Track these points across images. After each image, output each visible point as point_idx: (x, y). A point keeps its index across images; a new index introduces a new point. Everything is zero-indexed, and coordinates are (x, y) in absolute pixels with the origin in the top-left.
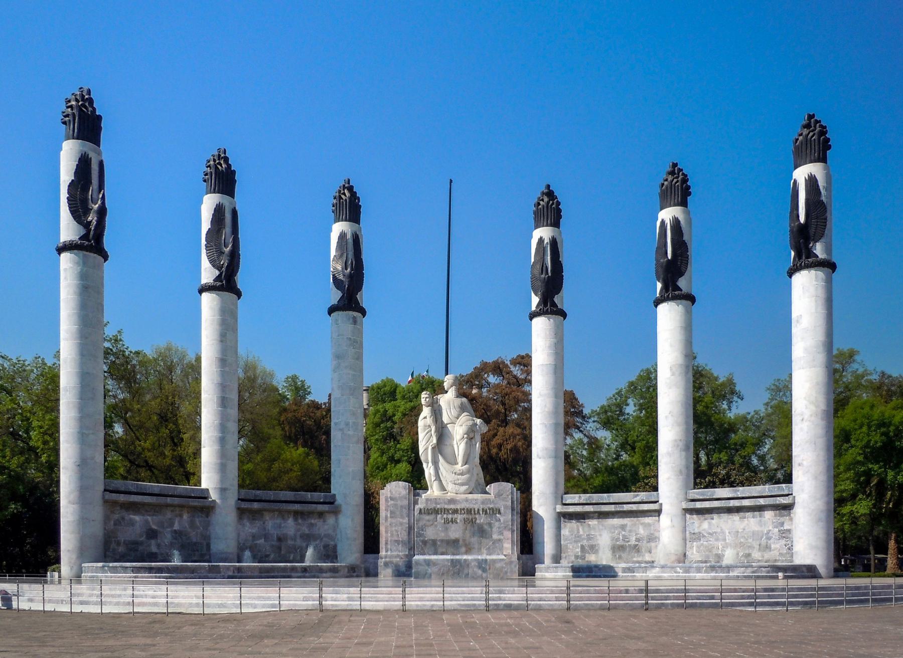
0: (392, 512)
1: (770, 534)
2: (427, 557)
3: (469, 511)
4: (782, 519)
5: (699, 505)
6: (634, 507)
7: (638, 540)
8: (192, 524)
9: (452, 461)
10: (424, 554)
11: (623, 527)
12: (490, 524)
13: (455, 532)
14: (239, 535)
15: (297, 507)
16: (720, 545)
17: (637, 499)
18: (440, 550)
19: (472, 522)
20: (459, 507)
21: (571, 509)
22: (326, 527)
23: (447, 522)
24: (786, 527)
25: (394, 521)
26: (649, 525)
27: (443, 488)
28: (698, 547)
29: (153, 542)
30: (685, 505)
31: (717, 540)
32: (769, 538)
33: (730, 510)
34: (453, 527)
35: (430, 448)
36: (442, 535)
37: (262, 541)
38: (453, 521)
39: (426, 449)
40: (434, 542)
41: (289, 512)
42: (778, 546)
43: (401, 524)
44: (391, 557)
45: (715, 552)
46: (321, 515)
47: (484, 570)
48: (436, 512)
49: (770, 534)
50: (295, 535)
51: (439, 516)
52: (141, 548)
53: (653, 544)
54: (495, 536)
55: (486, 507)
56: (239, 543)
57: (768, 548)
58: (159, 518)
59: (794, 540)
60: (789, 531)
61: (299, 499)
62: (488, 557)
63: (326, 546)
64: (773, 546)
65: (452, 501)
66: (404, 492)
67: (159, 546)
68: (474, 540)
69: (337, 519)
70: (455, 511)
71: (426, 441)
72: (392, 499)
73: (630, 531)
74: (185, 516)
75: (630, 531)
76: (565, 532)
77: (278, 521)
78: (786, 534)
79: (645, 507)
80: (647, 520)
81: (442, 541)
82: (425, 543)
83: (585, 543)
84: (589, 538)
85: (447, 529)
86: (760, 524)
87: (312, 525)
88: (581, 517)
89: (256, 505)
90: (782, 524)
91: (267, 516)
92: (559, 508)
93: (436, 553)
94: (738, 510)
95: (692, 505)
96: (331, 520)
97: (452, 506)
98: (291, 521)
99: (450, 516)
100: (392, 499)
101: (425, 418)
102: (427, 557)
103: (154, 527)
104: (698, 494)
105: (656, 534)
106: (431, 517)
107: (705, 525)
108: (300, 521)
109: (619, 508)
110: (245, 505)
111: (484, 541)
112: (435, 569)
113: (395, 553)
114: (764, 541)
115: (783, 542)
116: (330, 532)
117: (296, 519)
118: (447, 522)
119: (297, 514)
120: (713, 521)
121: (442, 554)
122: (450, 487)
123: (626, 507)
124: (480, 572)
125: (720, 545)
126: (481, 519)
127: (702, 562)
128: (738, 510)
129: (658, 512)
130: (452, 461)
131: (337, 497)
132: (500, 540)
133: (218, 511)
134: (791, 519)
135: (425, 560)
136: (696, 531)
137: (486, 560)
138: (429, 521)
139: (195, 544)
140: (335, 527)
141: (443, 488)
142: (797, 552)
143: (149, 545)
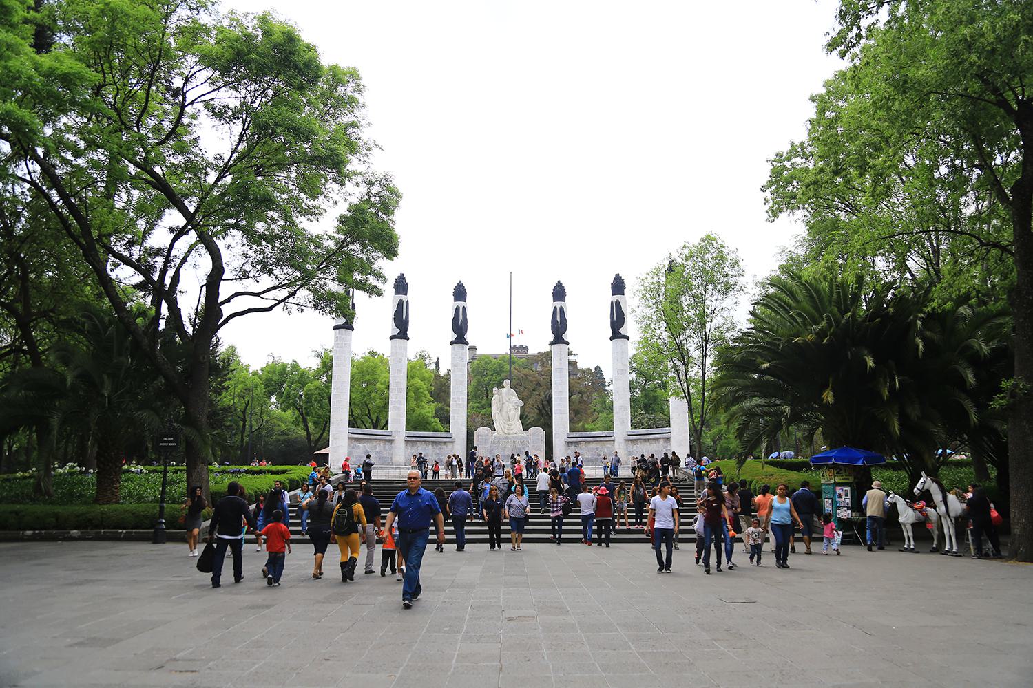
3: (514, 442)
8: (384, 447)
11: (597, 449)
14: (405, 453)
39: (495, 414)
41: (429, 442)
58: (370, 445)
71: (494, 410)
72: (481, 436)
77: (425, 446)
79: (607, 439)
80: (609, 445)
88: (577, 444)
89: (414, 439)
94: (649, 439)
96: (450, 446)
98: (430, 446)
100: (481, 436)
110: (409, 439)
117: (433, 446)
129: (614, 441)
133: (396, 441)
134: (670, 444)
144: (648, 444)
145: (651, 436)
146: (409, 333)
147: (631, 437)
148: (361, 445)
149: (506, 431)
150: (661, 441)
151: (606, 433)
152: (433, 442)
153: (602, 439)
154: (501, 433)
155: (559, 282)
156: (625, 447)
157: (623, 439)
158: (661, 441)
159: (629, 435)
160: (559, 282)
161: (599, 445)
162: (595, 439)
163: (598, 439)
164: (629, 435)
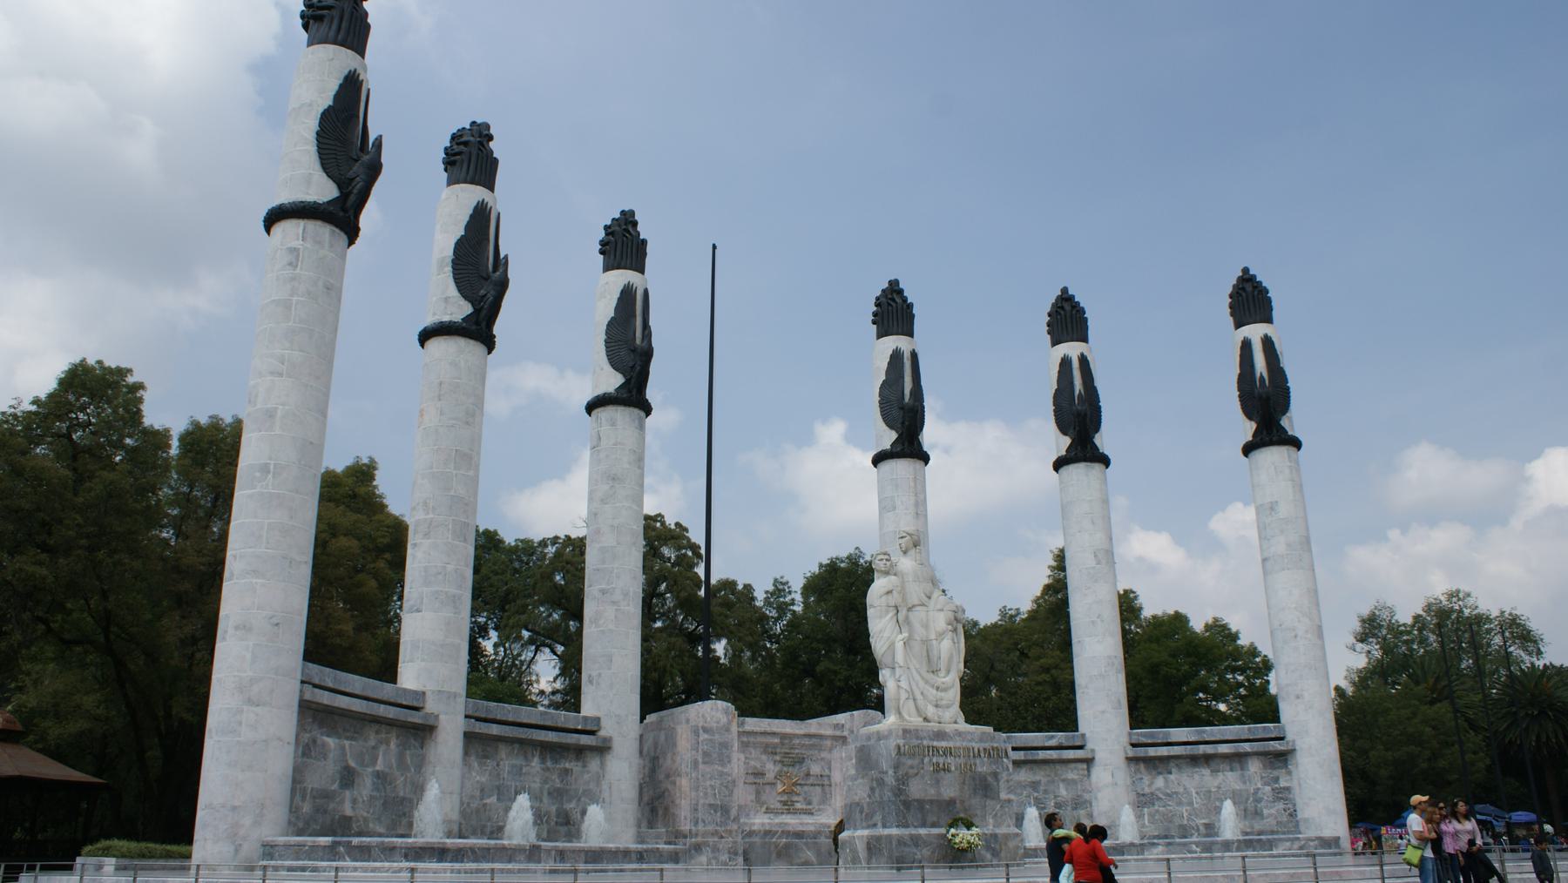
0: (706, 754)
1: (1260, 795)
2: (913, 831)
4: (1276, 773)
5: (1152, 752)
6: (1053, 754)
7: (1058, 805)
10: (906, 826)
12: (995, 775)
13: (949, 790)
15: (551, 737)
16: (1184, 810)
17: (1053, 743)
18: (931, 818)
20: (951, 744)
22: (586, 776)
24: (1283, 784)
25: (708, 769)
26: (1074, 782)
28: (1151, 815)
29: (348, 793)
30: (1131, 752)
31: (1180, 803)
32: (1258, 800)
33: (1194, 760)
35: (899, 646)
36: (932, 793)
37: (493, 799)
38: (946, 770)
39: (892, 646)
40: (921, 803)
42: (1273, 811)
43: (721, 774)
44: (705, 834)
45: (1177, 821)
46: (580, 752)
47: (996, 854)
49: (1260, 795)
50: (541, 790)
51: (926, 760)
52: (331, 806)
53: (1082, 812)
54: (1003, 796)
55: (987, 745)
56: (462, 803)
57: (1257, 814)
59: (1299, 801)
60: (1288, 789)
61: (548, 723)
62: (997, 831)
64: (1265, 812)
66: (724, 720)
67: (354, 801)
68: (976, 801)
69: (602, 765)
70: (948, 752)
72: (705, 730)
73: (1046, 792)
74: (393, 746)
75: (1046, 792)
77: (519, 761)
78: (1282, 794)
79: (1071, 754)
80: (1072, 774)
81: (931, 802)
82: (907, 804)
85: (938, 781)
86: (1244, 780)
87: (567, 772)
89: (495, 730)
90: (1277, 780)
91: (503, 751)
93: (924, 825)
94: (1207, 759)
95: (1141, 752)
96: (594, 764)
97: (944, 744)
99: (941, 760)
100: (705, 730)
102: (913, 831)
103: (352, 764)
104: (1144, 735)
105: (1087, 796)
106: (916, 762)
107: (1160, 782)
108: (549, 764)
109: (1030, 755)
111: (989, 802)
112: (926, 852)
113: (710, 828)
114: (1250, 805)
115: (1281, 806)
116: (592, 786)
117: (543, 760)
118: (938, 769)
119: (547, 749)
120: (1172, 777)
121: (934, 825)
123: (1042, 755)
124: (989, 856)
125: (1184, 810)
126: (983, 767)
127: (1158, 837)
128: (1207, 759)
129: (1089, 762)
131: (603, 723)
132: (1009, 801)
135: (912, 837)
136: (1147, 790)
137: (995, 836)
138: (912, 767)
139: (404, 799)
140: (598, 779)
142: (1306, 820)
143: (342, 802)
144: (1206, 772)
145: (1224, 749)
146: (502, 327)
147: (1152, 752)
148: (331, 742)
149: (931, 711)
150: (1254, 766)
151: (1059, 737)
152: (547, 749)
153: (1053, 754)
154: (915, 721)
156: (1129, 782)
157: (1122, 756)
158: (1254, 766)
159: (1134, 745)
161: (1040, 775)
162: (1030, 755)
163: (1042, 755)
164: (1134, 745)
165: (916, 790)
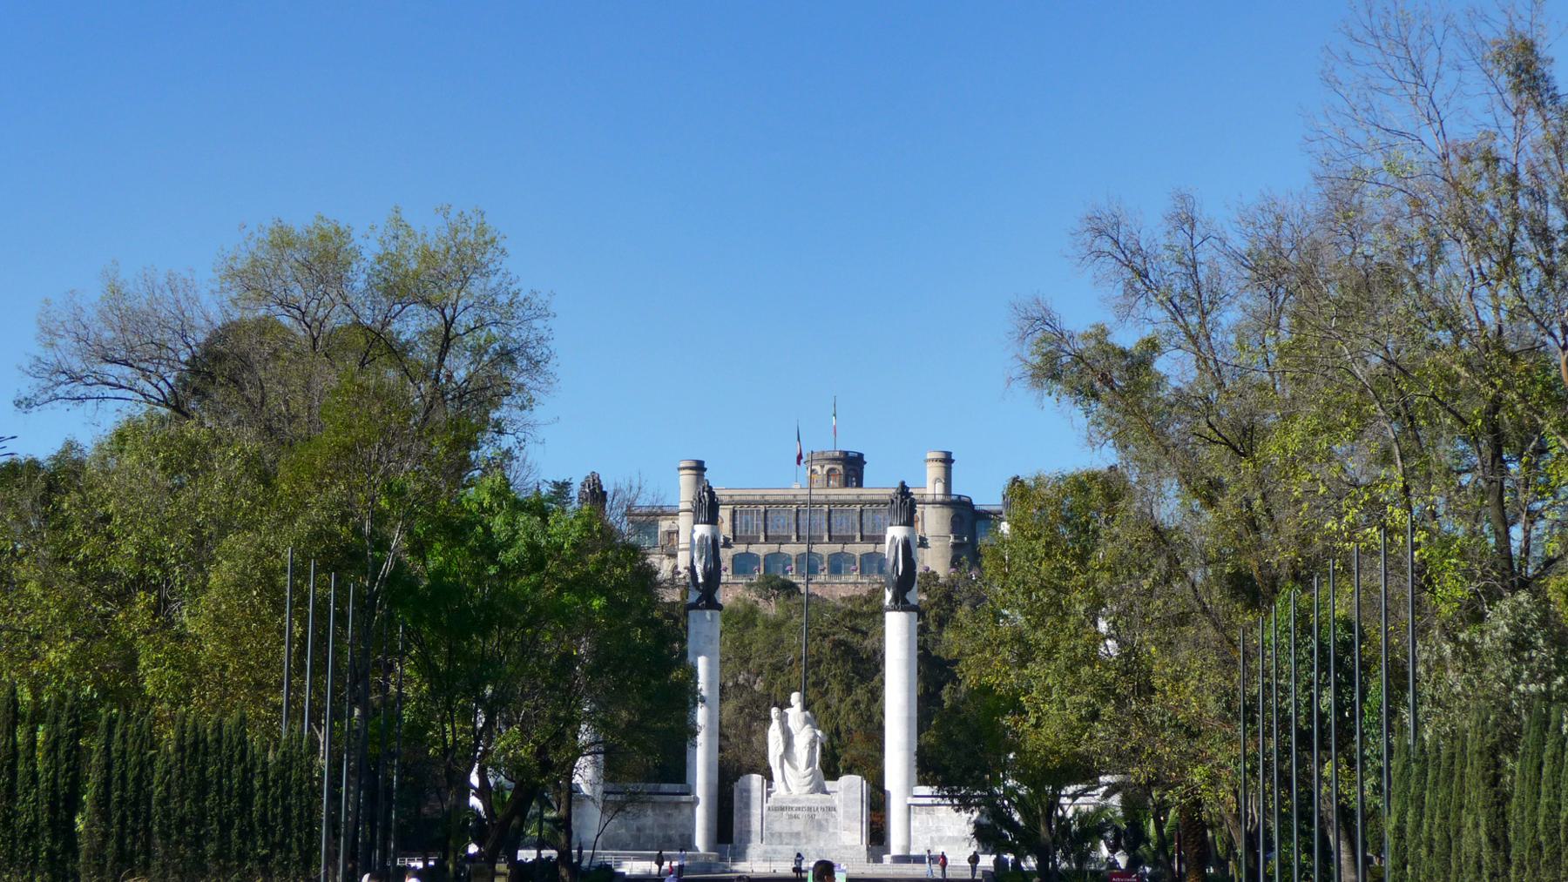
3: (810, 809)
9: (795, 768)
13: (798, 826)
19: (812, 817)
21: (921, 801)
23: (791, 817)
27: (788, 789)
34: (796, 821)
36: (786, 829)
38: (796, 817)
40: (780, 834)
48: (782, 809)
63: (681, 836)
65: (794, 801)
68: (813, 833)
76: (915, 824)
83: (934, 834)
84: (938, 830)
92: (910, 800)
101: (774, 734)
118: (791, 817)
122: (795, 791)
126: (819, 816)
130: (795, 768)
141: (788, 789)
155: (903, 484)
160: (903, 484)
165: (777, 827)
